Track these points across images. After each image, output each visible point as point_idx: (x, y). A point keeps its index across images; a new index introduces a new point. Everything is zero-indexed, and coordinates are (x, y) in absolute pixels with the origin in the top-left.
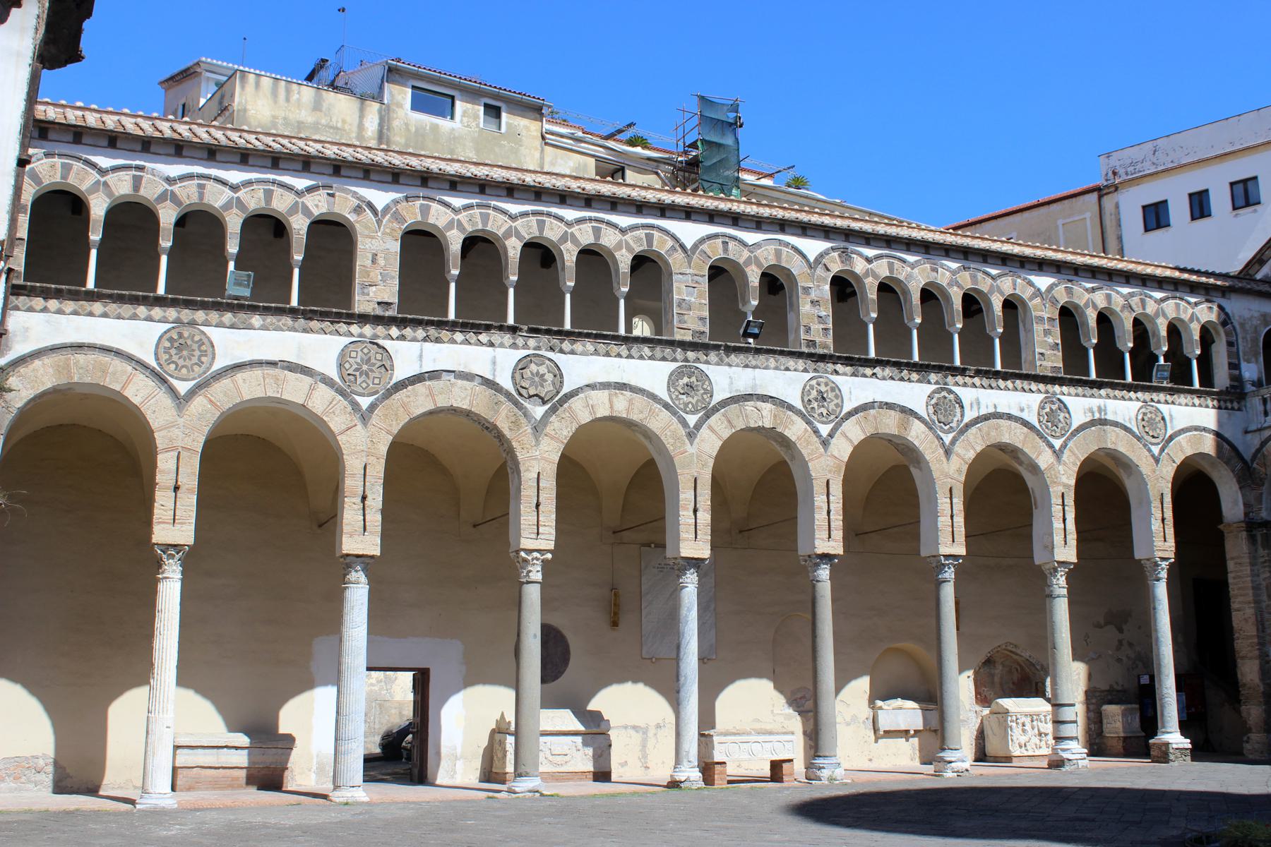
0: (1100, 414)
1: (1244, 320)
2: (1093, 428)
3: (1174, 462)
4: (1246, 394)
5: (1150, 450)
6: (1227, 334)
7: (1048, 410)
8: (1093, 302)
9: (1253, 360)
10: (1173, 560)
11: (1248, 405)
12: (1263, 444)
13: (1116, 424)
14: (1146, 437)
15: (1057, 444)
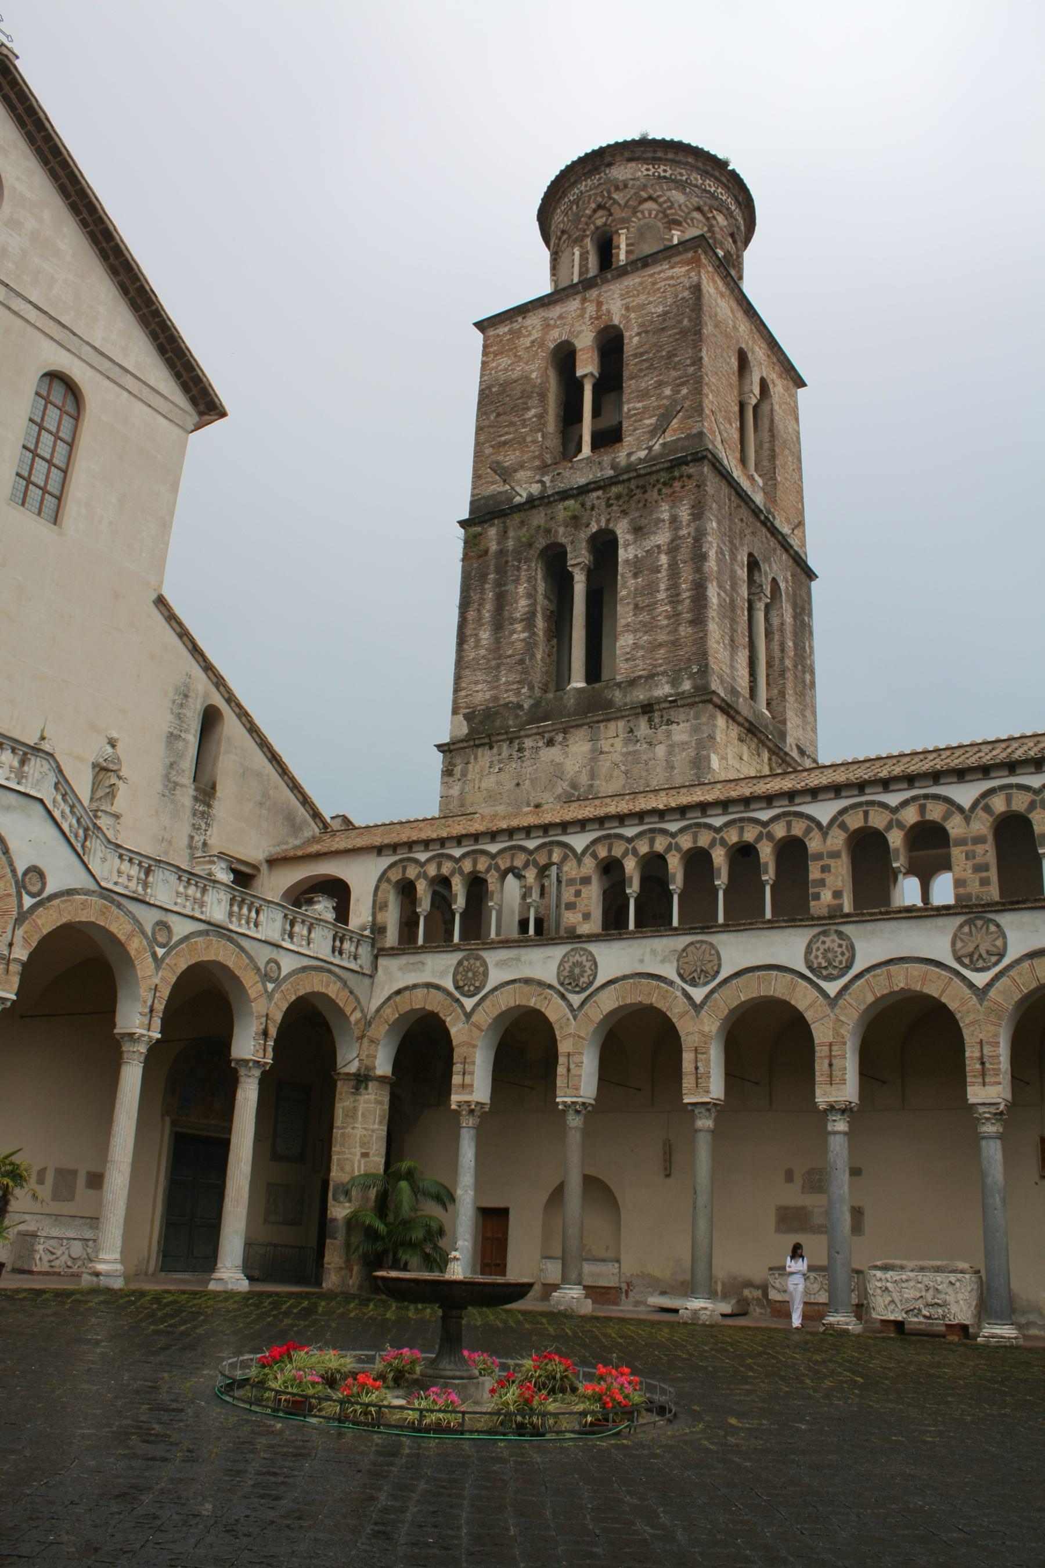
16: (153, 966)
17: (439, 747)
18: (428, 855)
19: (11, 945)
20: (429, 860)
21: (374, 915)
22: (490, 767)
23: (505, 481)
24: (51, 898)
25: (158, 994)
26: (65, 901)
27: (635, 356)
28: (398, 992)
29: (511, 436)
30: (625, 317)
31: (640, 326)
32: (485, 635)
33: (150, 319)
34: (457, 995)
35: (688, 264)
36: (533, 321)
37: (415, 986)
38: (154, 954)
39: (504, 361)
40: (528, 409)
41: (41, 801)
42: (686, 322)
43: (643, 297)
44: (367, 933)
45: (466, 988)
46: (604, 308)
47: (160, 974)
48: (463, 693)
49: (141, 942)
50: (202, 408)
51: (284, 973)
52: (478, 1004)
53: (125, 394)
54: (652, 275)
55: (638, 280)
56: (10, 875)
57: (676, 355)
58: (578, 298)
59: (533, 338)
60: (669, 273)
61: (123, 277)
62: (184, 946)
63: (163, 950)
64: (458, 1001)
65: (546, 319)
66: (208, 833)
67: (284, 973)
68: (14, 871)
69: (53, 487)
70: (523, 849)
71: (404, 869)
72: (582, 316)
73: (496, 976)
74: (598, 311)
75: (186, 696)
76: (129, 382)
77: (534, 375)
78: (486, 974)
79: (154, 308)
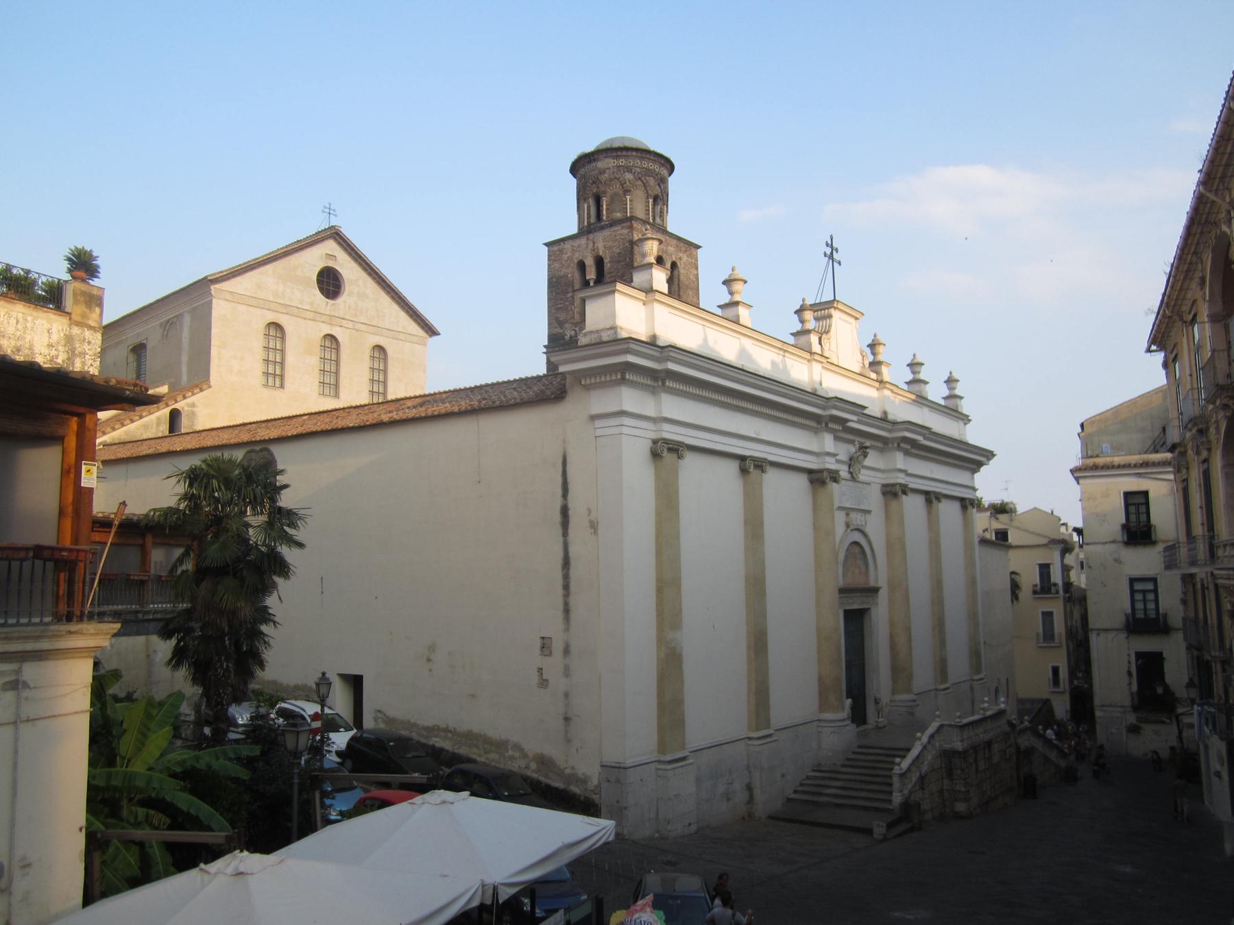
23: (561, 328)
27: (610, 273)
29: (562, 305)
30: (604, 252)
31: (610, 258)
35: (628, 229)
36: (567, 246)
39: (557, 265)
40: (568, 293)
42: (628, 259)
43: (611, 243)
46: (596, 245)
50: (430, 333)
53: (400, 342)
54: (614, 231)
55: (609, 233)
57: (624, 276)
58: (585, 237)
59: (568, 255)
60: (620, 232)
61: (392, 294)
65: (573, 246)
72: (587, 248)
74: (594, 246)
76: (401, 336)
77: (569, 276)
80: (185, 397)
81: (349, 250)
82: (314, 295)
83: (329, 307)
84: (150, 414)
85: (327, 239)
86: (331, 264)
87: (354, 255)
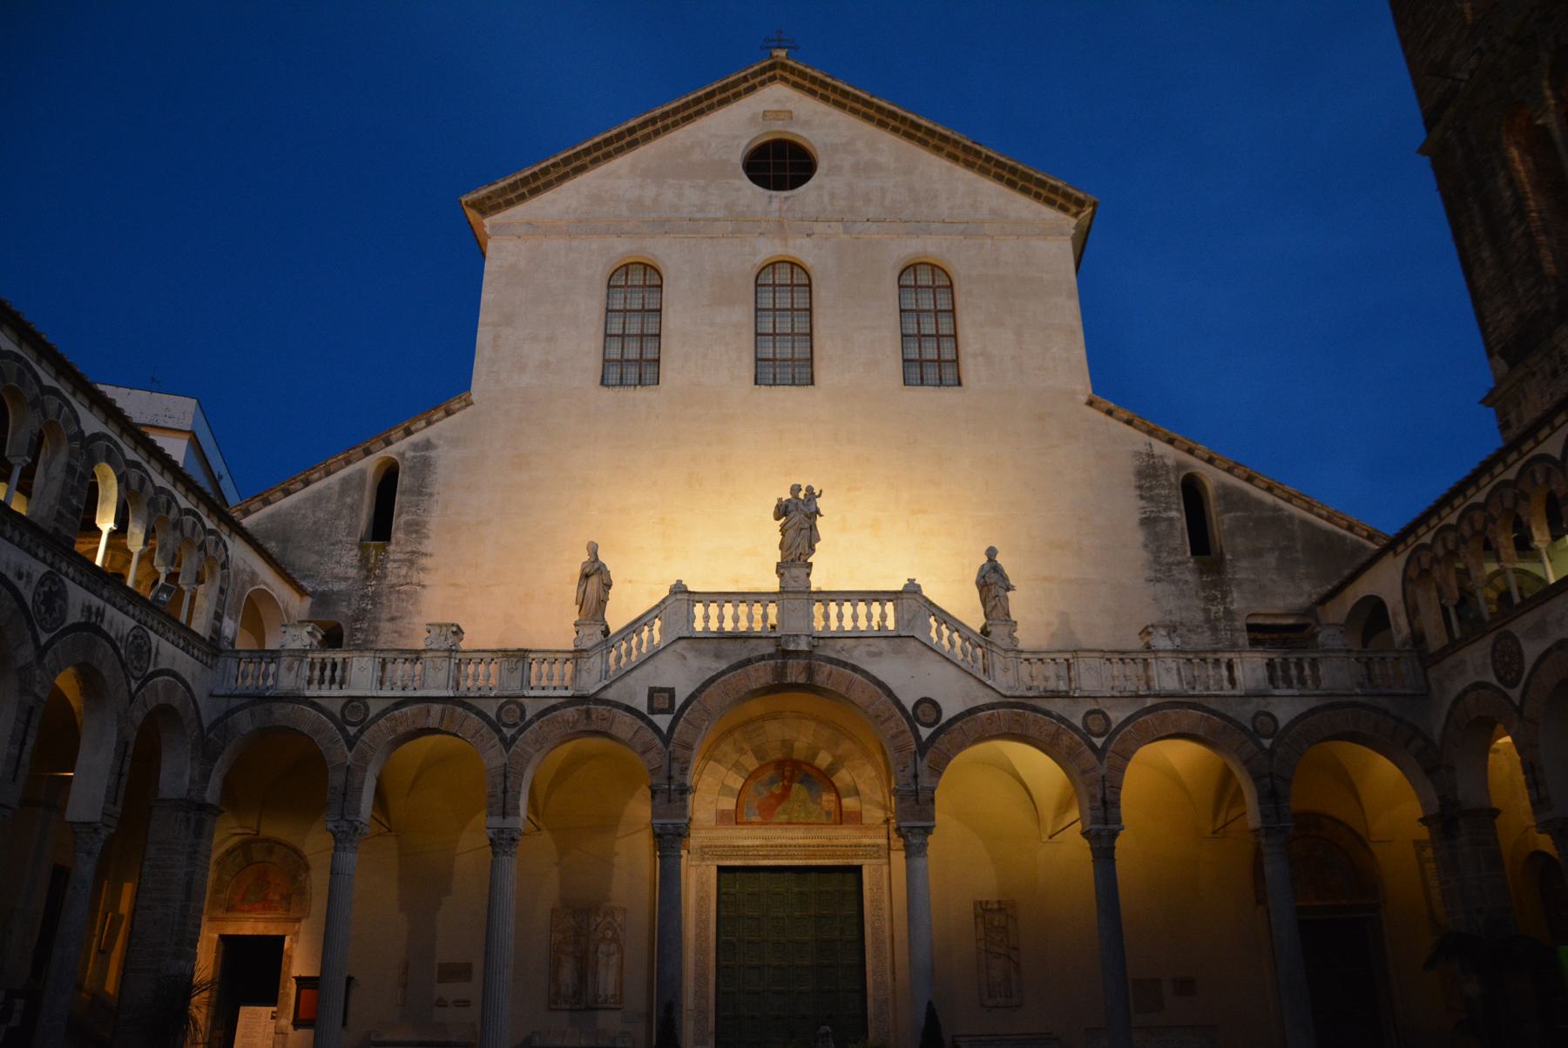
0: (97, 617)
1: (238, 570)
2: (85, 634)
3: (146, 707)
4: (221, 651)
5: (129, 684)
6: (223, 579)
7: (46, 589)
8: (127, 478)
9: (234, 617)
10: (113, 831)
11: (221, 665)
12: (230, 712)
13: (107, 637)
14: (129, 666)
15: (44, 638)
16: (1094, 758)
17: (1482, 402)
18: (1432, 533)
19: (916, 776)
20: (1434, 539)
21: (1411, 624)
22: (1542, 398)
24: (951, 722)
25: (1107, 784)
26: (968, 721)
28: (1455, 702)
32: (1485, 254)
33: (987, 165)
34: (1502, 687)
37: (1465, 692)
38: (1092, 746)
41: (913, 637)
44: (1407, 648)
45: (1509, 678)
47: (1105, 762)
48: (1490, 329)
49: (1072, 738)
50: (1074, 209)
51: (1282, 724)
52: (1524, 694)
56: (899, 715)
61: (949, 148)
62: (1129, 728)
63: (1103, 739)
64: (1506, 696)
66: (1228, 600)
67: (1282, 724)
68: (902, 709)
69: (948, 354)
70: (1506, 483)
71: (1419, 559)
73: (1532, 650)
75: (1156, 477)
78: (1520, 653)
79: (983, 156)
80: (408, 432)
81: (820, 91)
82: (738, 190)
83: (775, 205)
84: (328, 474)
85: (763, 83)
86: (779, 129)
87: (833, 96)
